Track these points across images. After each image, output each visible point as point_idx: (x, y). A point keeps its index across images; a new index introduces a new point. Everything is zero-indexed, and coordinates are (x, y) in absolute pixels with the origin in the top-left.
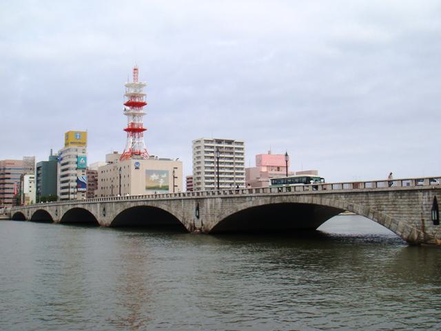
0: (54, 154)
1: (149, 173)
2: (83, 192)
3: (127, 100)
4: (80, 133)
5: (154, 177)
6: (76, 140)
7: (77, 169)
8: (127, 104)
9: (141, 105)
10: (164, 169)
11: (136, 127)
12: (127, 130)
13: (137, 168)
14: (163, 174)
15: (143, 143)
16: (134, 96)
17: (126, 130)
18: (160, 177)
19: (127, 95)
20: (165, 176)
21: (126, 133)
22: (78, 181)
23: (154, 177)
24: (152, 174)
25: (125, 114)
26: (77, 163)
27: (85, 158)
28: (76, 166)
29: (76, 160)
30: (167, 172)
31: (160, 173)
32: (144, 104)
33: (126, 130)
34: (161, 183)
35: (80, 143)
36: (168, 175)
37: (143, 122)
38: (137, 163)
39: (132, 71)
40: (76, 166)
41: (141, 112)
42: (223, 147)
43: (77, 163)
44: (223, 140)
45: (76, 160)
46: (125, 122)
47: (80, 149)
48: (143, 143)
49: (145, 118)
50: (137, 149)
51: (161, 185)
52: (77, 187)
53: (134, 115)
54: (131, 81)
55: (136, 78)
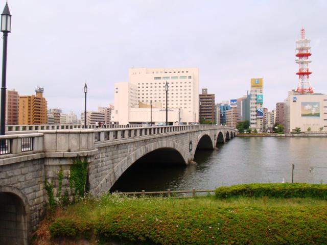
1: (304, 104)
2: (261, 118)
3: (297, 52)
4: (258, 80)
5: (308, 107)
6: (257, 84)
7: (256, 103)
9: (308, 55)
10: (316, 101)
11: (304, 71)
13: (295, 101)
15: (309, 82)
16: (302, 49)
17: (297, 74)
18: (313, 107)
19: (297, 49)
20: (316, 106)
21: (298, 76)
22: (257, 111)
23: (308, 107)
25: (297, 63)
26: (256, 99)
27: (262, 96)
28: (256, 101)
29: (255, 97)
30: (318, 103)
31: (312, 104)
32: (309, 55)
34: (314, 112)
35: (258, 86)
36: (319, 105)
38: (295, 98)
39: (300, 31)
40: (256, 101)
41: (308, 60)
43: (256, 99)
46: (297, 68)
47: (258, 90)
48: (309, 82)
49: (311, 65)
50: (306, 87)
51: (313, 113)
53: (302, 63)
54: (300, 39)
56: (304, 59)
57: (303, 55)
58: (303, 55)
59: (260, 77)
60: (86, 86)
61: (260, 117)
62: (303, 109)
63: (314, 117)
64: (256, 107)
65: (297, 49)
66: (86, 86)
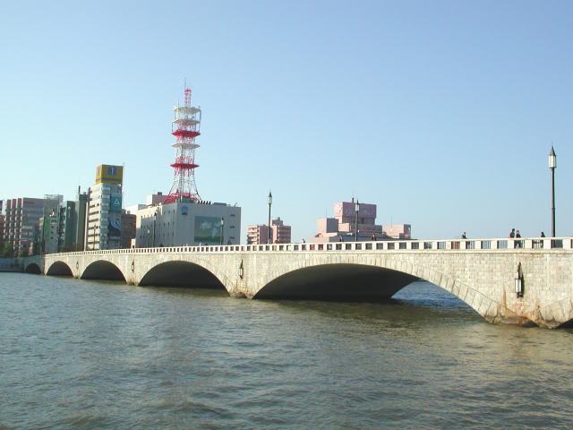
0: (82, 193)
3: (176, 128)
4: (115, 167)
5: (205, 225)
8: (177, 133)
11: (186, 161)
12: (176, 166)
16: (187, 122)
17: (173, 166)
18: (213, 226)
19: (177, 122)
21: (173, 169)
23: (205, 225)
24: (203, 222)
32: (196, 134)
33: (173, 166)
34: (214, 233)
37: (198, 157)
46: (174, 155)
51: (213, 236)
55: (188, 100)
56: (188, 140)
57: (186, 133)
58: (186, 133)
59: (120, 165)
60: (270, 196)
61: (115, 238)
65: (177, 122)
66: (270, 196)
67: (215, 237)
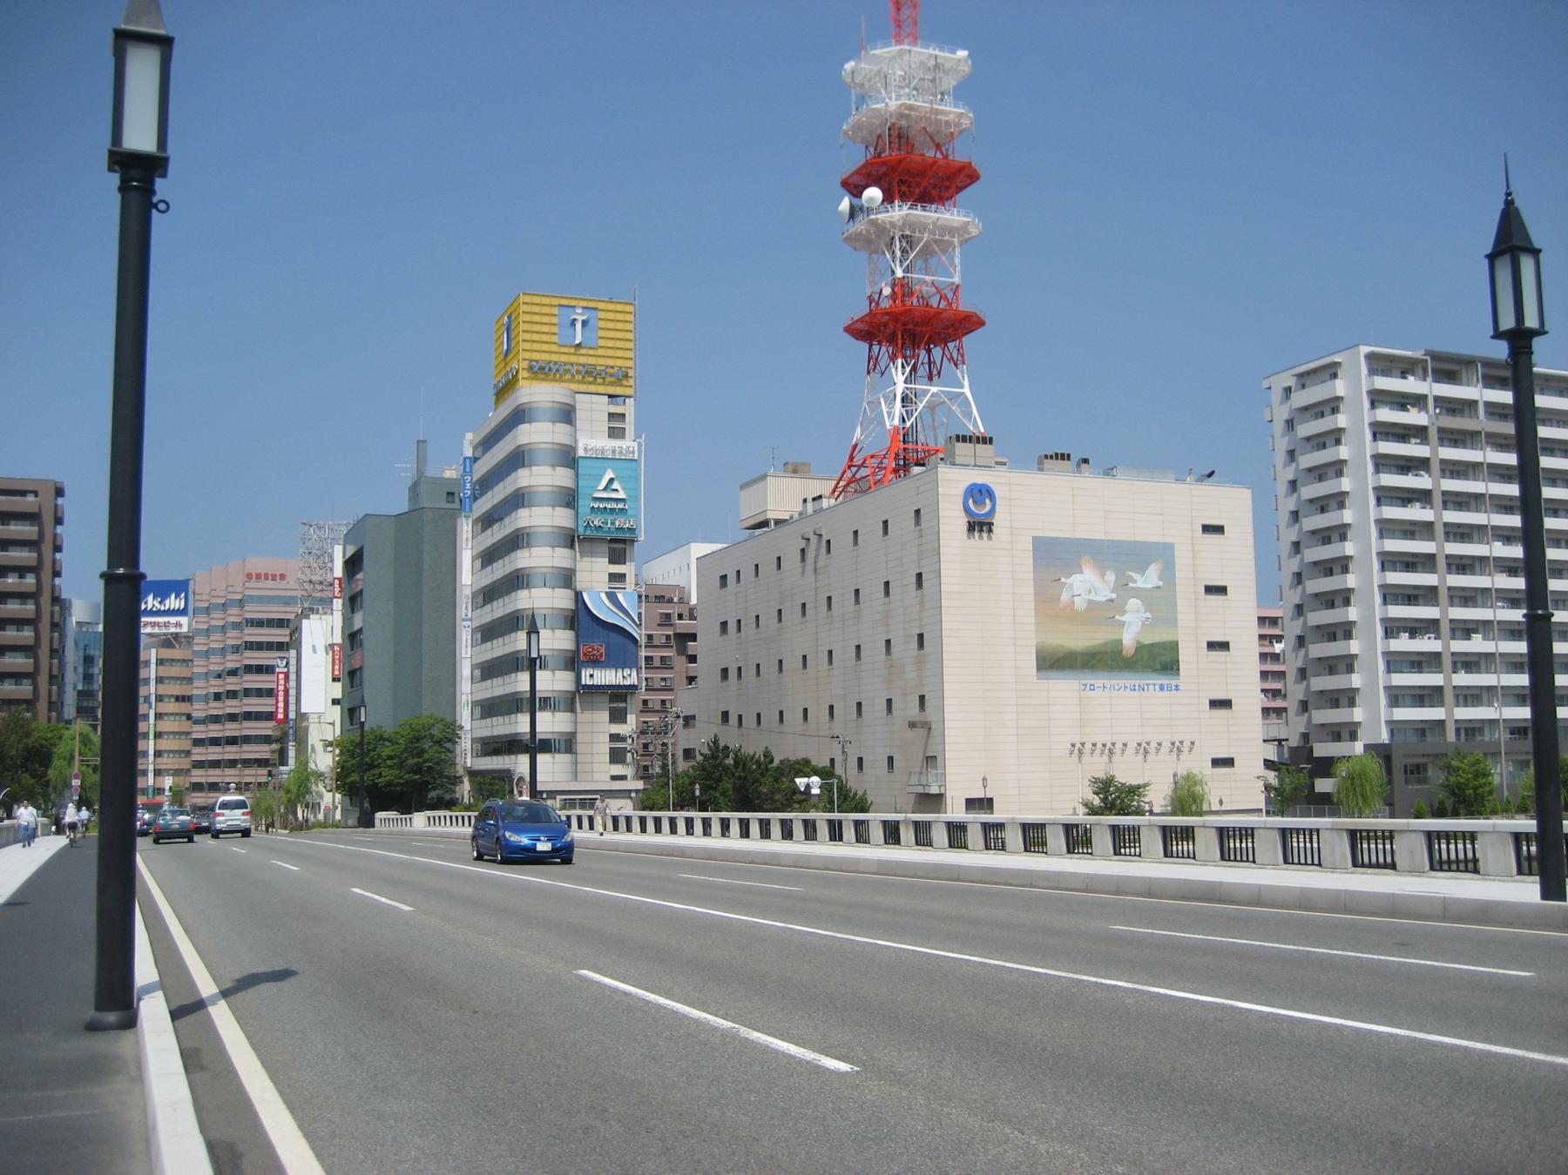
10: (1147, 533)
13: (979, 526)
14: (1142, 570)
18: (1123, 586)
20: (1149, 579)
22: (579, 618)
26: (569, 499)
28: (561, 517)
29: (562, 477)
30: (1163, 554)
34: (1132, 630)
36: (1168, 573)
38: (980, 493)
40: (561, 517)
42: (1472, 404)
43: (569, 499)
44: (1469, 362)
45: (562, 477)
52: (573, 662)
62: (1047, 601)
63: (1131, 680)
64: (567, 578)
67: (1140, 648)
